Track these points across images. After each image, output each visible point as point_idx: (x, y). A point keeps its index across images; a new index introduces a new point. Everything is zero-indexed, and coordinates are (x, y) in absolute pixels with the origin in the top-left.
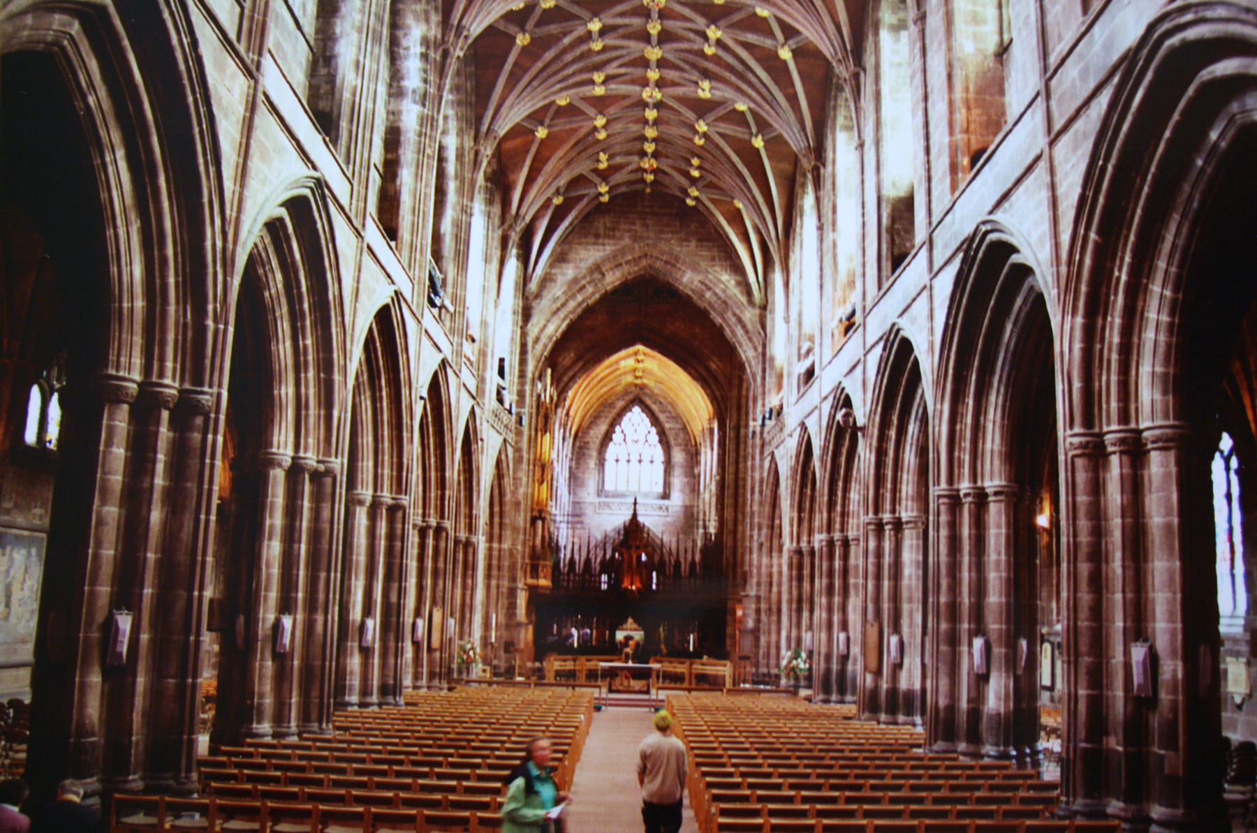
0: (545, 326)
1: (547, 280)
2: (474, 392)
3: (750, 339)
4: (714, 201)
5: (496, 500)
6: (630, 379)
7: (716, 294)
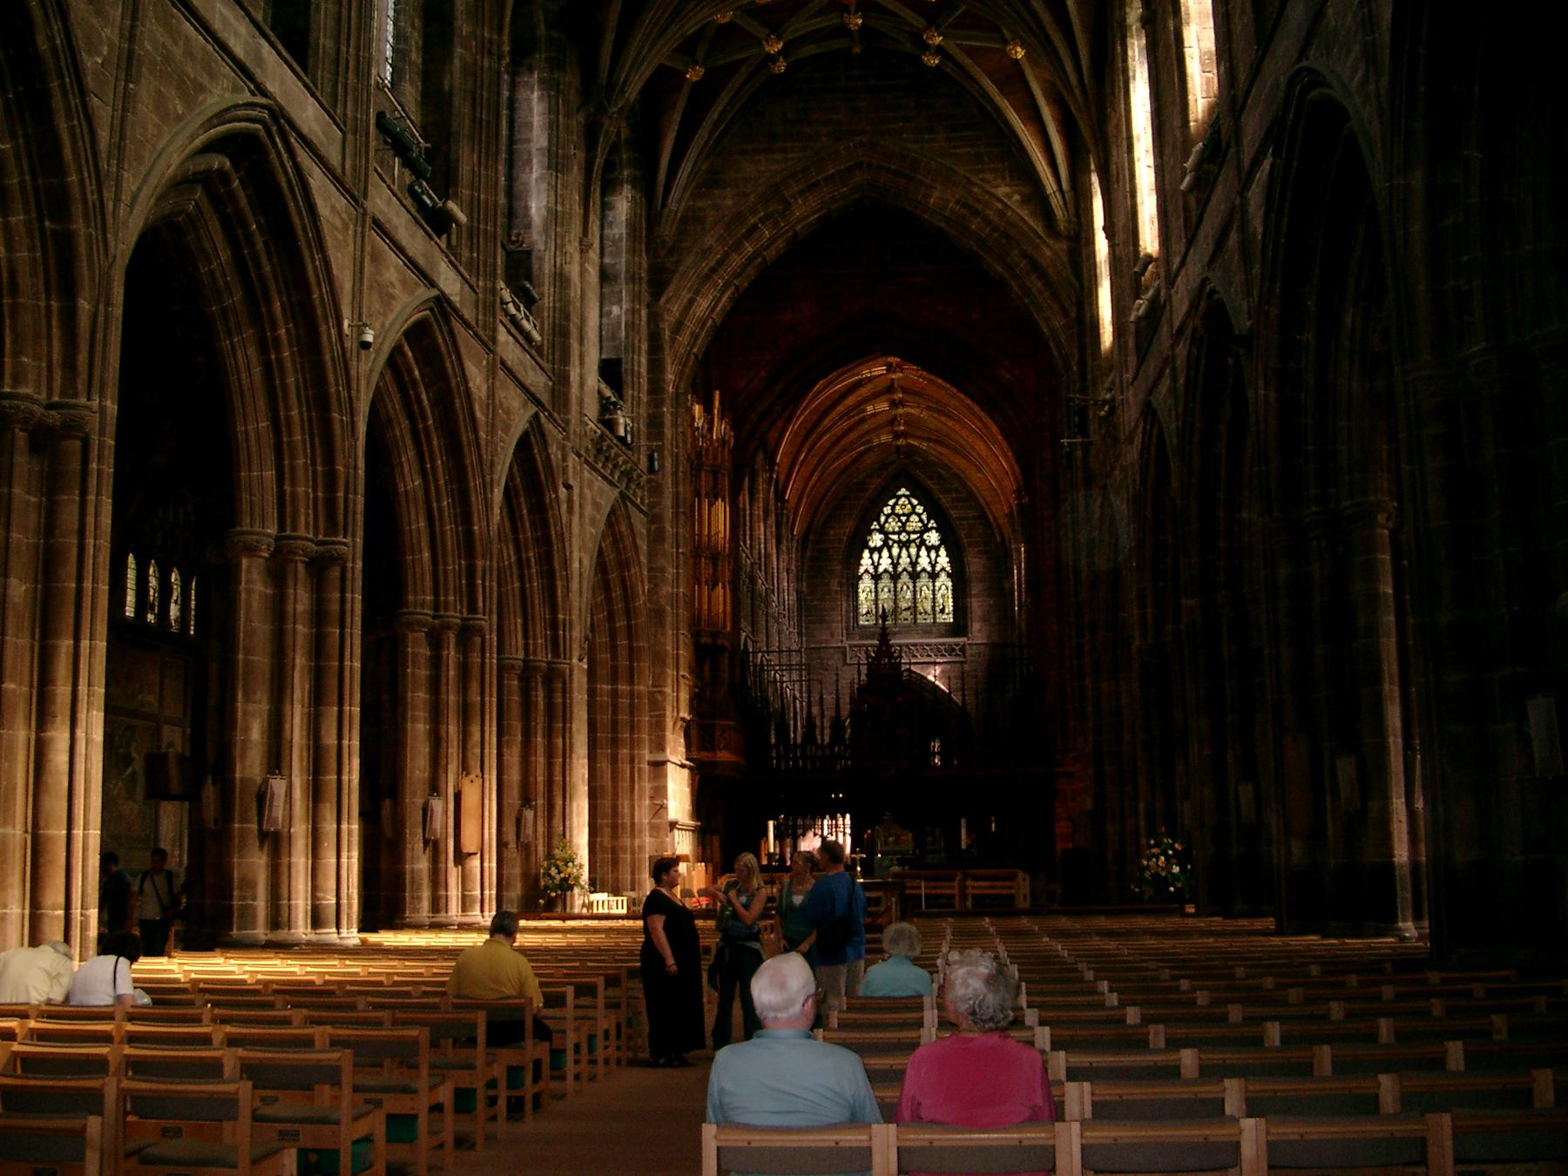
0: (691, 301)
1: (692, 219)
2: (545, 398)
3: (1055, 297)
4: (970, 52)
5: (619, 606)
6: (885, 438)
7: (988, 222)
